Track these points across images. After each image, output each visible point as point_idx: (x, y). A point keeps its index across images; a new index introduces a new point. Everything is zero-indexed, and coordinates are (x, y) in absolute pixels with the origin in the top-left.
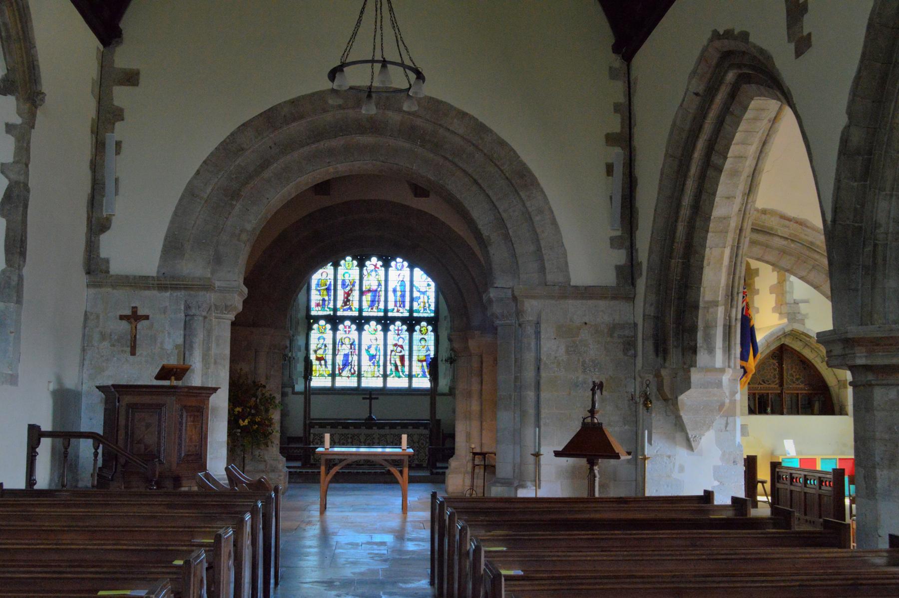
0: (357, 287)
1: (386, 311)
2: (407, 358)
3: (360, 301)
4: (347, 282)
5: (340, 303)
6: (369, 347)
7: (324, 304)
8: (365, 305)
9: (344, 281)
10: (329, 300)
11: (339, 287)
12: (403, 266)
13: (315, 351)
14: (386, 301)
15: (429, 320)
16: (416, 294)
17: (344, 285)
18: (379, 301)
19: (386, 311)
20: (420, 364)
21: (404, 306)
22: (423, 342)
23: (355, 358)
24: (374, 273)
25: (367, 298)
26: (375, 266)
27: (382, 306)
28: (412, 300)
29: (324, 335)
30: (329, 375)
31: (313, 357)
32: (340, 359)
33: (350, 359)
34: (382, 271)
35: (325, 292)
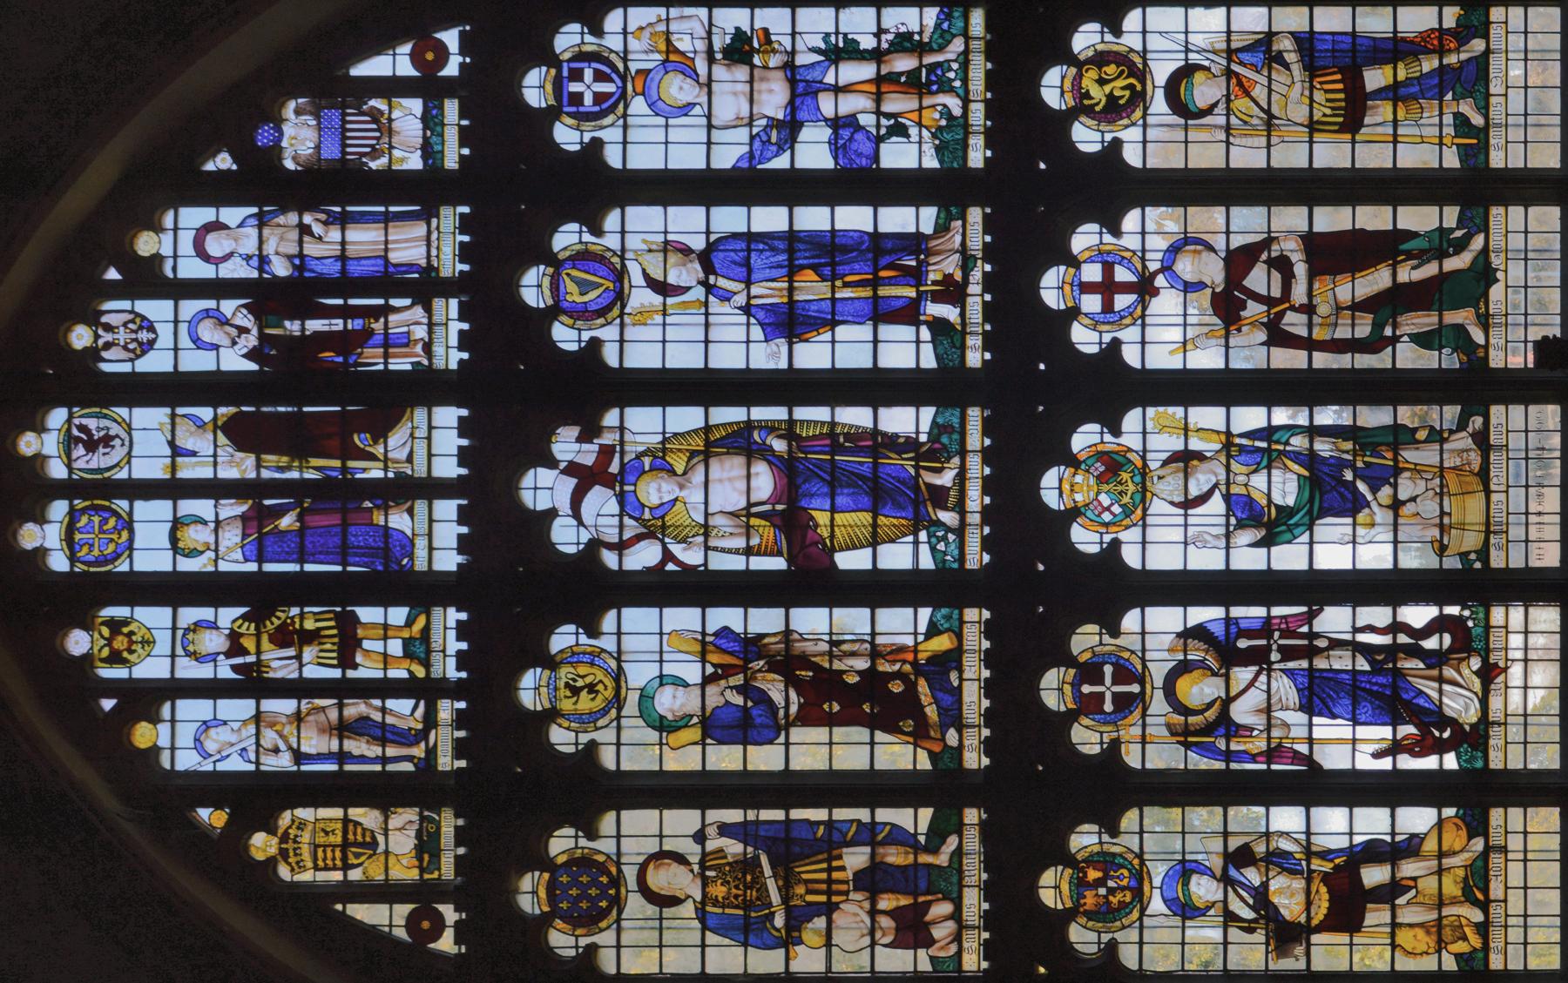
0: (765, 621)
1: (936, 387)
3: (879, 589)
5: (897, 755)
10: (869, 834)
11: (765, 758)
21: (914, 242)
22: (1204, 92)
23: (1335, 620)
28: (859, 181)
35: (811, 871)
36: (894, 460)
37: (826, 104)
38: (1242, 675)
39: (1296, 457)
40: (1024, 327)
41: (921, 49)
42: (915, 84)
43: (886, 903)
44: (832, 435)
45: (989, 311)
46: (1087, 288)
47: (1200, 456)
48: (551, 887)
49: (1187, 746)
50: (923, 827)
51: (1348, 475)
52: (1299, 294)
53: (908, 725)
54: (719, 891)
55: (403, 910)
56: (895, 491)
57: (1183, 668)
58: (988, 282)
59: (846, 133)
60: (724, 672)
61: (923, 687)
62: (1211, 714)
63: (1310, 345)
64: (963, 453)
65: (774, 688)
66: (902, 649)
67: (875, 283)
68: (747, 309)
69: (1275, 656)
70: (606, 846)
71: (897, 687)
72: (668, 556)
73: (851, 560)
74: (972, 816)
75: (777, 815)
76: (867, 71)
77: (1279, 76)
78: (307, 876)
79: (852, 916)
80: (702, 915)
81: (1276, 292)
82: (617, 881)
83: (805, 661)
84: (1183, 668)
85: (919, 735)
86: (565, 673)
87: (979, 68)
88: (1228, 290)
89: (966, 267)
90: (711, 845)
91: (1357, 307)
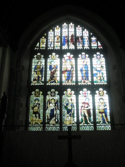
0: (59, 69)
1: (77, 82)
2: (92, 111)
3: (61, 77)
4: (53, 66)
5: (48, 78)
6: (67, 105)
7: (39, 80)
8: (64, 79)
9: (51, 66)
10: (42, 77)
11: (48, 69)
12: (86, 57)
13: (33, 108)
14: (77, 77)
15: (104, 87)
16: (95, 72)
17: (51, 68)
18: (72, 77)
19: (77, 82)
20: (101, 115)
21: (88, 79)
22: (101, 101)
23: (58, 111)
24: (69, 61)
25: (64, 76)
26: (69, 57)
27: (74, 79)
28: (92, 75)
29: (38, 98)
30: (41, 124)
31: (31, 111)
32: (48, 112)
33: (55, 112)
34: (73, 60)
35: (39, 72)
36: (71, 78)
37: (99, 73)
38: (54, 104)
39: (72, 108)
40: (81, 87)
41: (103, 79)
42: (100, 79)
43: (37, 78)
44: (73, 74)
45: (83, 85)
46: (85, 92)
47: (72, 101)
48: (39, 55)
49: (48, 100)
50: (42, 80)
51: (70, 113)
52: (85, 108)
53: (50, 79)
54: (38, 66)
55: (38, 46)
56: (68, 78)
57: (55, 100)
58: (85, 85)
59: (96, 74)
60: (55, 67)
61: (53, 80)
62: (51, 102)
63: (81, 110)
64: (72, 83)
65: (54, 70)
66: (56, 79)
67: (85, 76)
68: (82, 68)
69: (55, 107)
70: (42, 59)
71: (53, 78)
72: (63, 62)
73: (63, 75)
74: (43, 84)
75: (44, 70)
76: (101, 76)
77: (103, 107)
78: (41, 40)
79: (36, 76)
80: (37, 65)
81: (85, 107)
82: (39, 59)
83: (56, 72)
84: (55, 100)
85: (50, 80)
86: (55, 56)
87: (102, 84)
88: (85, 103)
89: (86, 83)
90: (42, 66)
91: (84, 113)
